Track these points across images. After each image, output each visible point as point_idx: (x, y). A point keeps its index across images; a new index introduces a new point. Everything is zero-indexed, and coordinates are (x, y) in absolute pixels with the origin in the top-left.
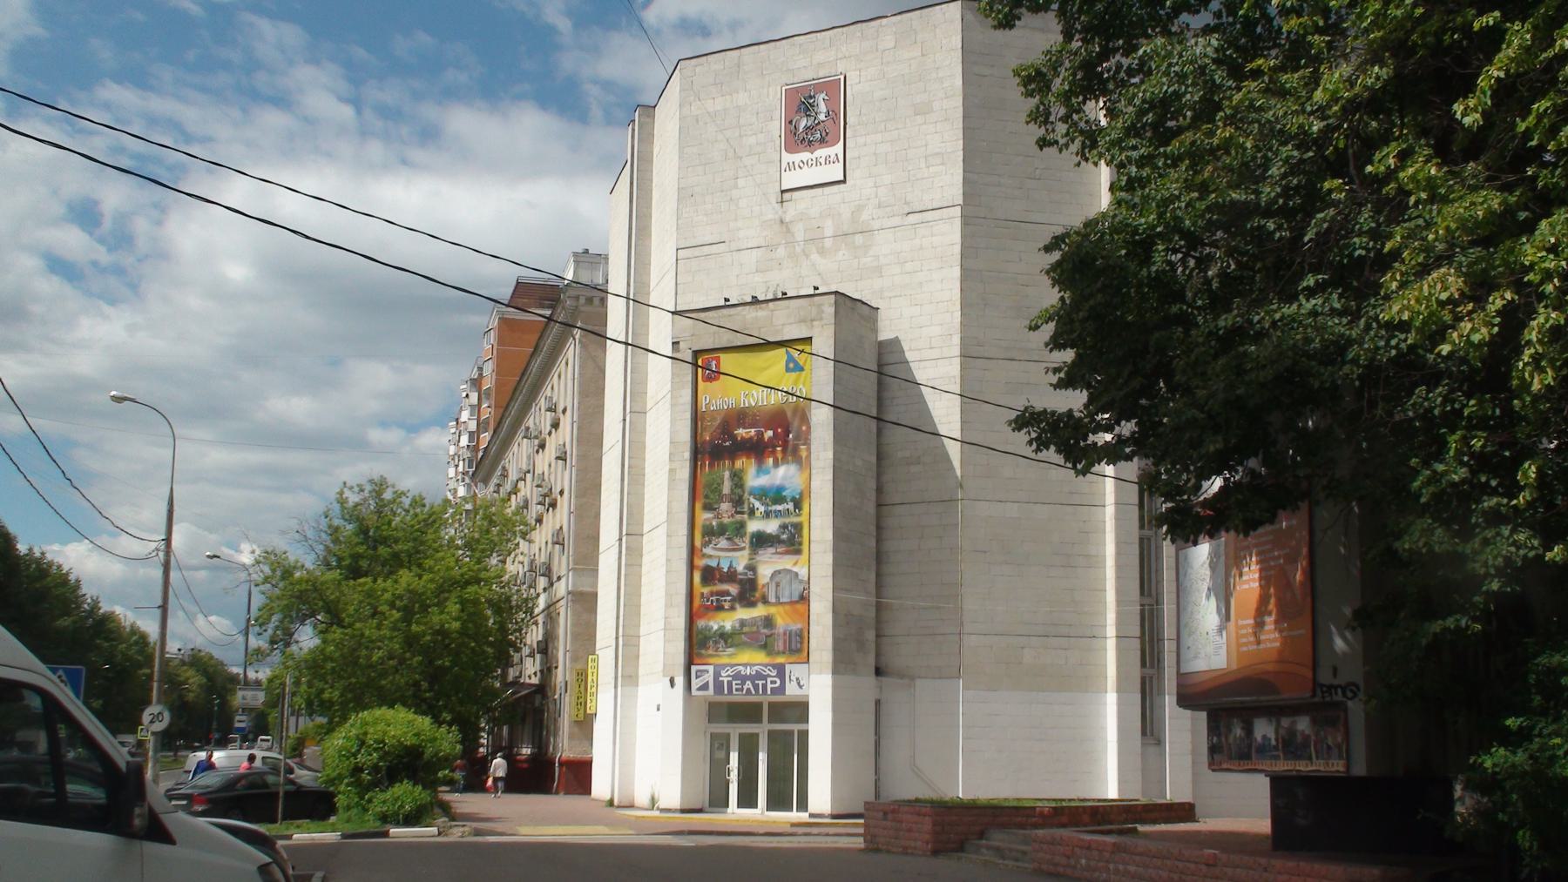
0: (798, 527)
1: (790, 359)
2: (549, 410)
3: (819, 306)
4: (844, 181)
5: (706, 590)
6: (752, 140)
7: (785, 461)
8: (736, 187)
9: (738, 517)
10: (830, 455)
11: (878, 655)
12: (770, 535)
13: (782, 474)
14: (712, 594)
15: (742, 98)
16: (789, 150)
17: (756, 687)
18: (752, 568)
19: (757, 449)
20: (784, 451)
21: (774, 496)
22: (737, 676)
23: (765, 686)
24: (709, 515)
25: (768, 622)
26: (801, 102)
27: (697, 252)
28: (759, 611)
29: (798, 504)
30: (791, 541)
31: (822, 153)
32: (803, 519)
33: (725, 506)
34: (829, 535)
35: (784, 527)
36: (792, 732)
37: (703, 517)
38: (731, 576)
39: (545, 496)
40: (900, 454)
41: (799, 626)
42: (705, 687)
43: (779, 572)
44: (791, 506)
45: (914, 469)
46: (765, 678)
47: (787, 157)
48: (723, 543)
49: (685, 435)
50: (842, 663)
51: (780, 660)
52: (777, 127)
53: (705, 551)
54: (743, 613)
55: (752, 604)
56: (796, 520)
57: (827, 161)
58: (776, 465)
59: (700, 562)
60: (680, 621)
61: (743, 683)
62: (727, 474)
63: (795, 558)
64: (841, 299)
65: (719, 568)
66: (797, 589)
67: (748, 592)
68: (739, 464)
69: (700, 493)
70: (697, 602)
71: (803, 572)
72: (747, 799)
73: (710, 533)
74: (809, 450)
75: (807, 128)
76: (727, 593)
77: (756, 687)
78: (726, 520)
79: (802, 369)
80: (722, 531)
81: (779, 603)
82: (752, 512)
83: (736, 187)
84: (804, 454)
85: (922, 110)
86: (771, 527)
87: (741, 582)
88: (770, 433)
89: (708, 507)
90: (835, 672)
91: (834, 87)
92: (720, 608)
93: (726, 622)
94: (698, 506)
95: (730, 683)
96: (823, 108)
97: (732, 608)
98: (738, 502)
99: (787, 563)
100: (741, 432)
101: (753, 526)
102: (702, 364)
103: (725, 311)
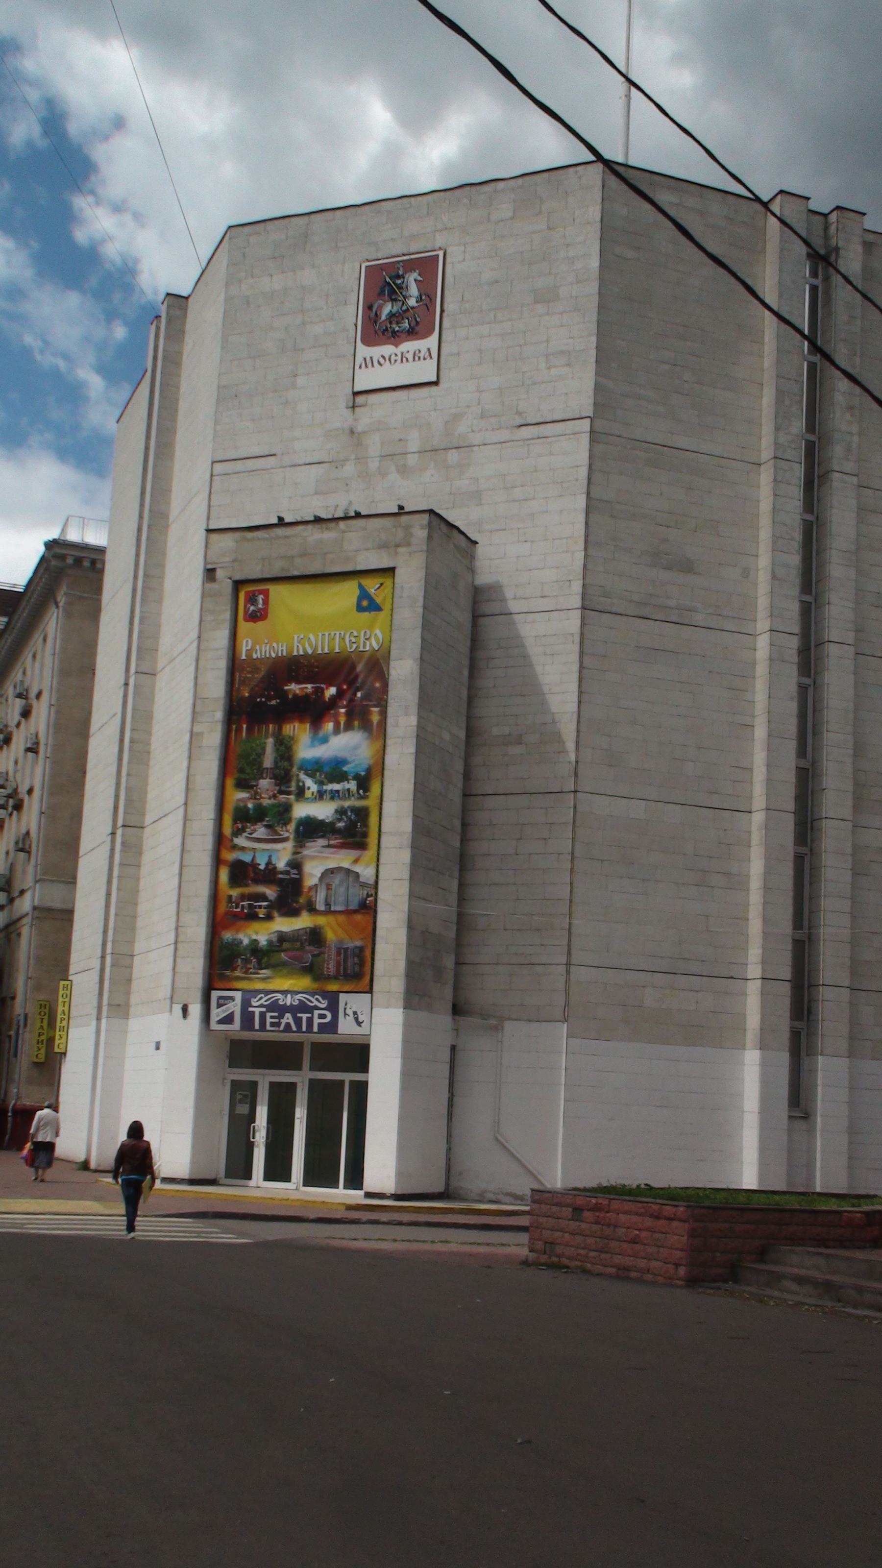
0: (362, 814)
1: (364, 594)
2: (19, 696)
3: (407, 528)
5: (235, 893)
6: (318, 329)
7: (349, 727)
8: (294, 386)
9: (282, 798)
10: (413, 720)
11: (456, 988)
12: (322, 823)
13: (344, 744)
14: (243, 897)
15: (308, 276)
16: (368, 341)
17: (298, 1021)
18: (296, 865)
19: (314, 712)
20: (350, 715)
21: (332, 771)
22: (273, 1007)
23: (310, 1021)
24: (243, 795)
25: (315, 936)
26: (384, 282)
27: (239, 466)
28: (303, 922)
29: (364, 783)
30: (354, 831)
31: (409, 346)
32: (371, 802)
33: (265, 784)
34: (407, 825)
35: (341, 812)
36: (342, 1082)
37: (236, 796)
38: (269, 875)
39: (9, 796)
40: (495, 731)
41: (358, 943)
42: (228, 1019)
43: (331, 871)
44: (352, 785)
45: (514, 750)
46: (310, 1010)
47: (363, 351)
48: (261, 831)
49: (216, 687)
50: (415, 996)
51: (333, 987)
52: (352, 313)
53: (240, 841)
54: (283, 925)
55: (293, 913)
56: (359, 803)
57: (416, 356)
58: (337, 731)
59: (230, 856)
60: (197, 930)
61: (281, 1016)
62: (270, 741)
63: (353, 854)
64: (433, 517)
65: (254, 865)
66: (357, 895)
67: (290, 894)
68: (289, 729)
69: (237, 767)
70: (223, 908)
71: (366, 872)
72: (278, 1169)
73: (245, 818)
74: (384, 714)
75: (391, 315)
76: (263, 897)
77: (298, 1021)
78: (266, 802)
79: (379, 609)
80: (259, 815)
81: (328, 912)
82: (301, 793)
83: (294, 386)
84: (375, 718)
85: (546, 297)
86: (323, 811)
87: (280, 883)
88: (333, 690)
89: (242, 785)
90: (408, 1005)
91: (427, 266)
92: (252, 917)
93: (261, 934)
94: (230, 782)
95: (263, 1016)
96: (414, 290)
97: (269, 918)
98: (283, 777)
99: (343, 859)
100: (294, 688)
101: (301, 811)
102: (248, 596)
103: (280, 531)
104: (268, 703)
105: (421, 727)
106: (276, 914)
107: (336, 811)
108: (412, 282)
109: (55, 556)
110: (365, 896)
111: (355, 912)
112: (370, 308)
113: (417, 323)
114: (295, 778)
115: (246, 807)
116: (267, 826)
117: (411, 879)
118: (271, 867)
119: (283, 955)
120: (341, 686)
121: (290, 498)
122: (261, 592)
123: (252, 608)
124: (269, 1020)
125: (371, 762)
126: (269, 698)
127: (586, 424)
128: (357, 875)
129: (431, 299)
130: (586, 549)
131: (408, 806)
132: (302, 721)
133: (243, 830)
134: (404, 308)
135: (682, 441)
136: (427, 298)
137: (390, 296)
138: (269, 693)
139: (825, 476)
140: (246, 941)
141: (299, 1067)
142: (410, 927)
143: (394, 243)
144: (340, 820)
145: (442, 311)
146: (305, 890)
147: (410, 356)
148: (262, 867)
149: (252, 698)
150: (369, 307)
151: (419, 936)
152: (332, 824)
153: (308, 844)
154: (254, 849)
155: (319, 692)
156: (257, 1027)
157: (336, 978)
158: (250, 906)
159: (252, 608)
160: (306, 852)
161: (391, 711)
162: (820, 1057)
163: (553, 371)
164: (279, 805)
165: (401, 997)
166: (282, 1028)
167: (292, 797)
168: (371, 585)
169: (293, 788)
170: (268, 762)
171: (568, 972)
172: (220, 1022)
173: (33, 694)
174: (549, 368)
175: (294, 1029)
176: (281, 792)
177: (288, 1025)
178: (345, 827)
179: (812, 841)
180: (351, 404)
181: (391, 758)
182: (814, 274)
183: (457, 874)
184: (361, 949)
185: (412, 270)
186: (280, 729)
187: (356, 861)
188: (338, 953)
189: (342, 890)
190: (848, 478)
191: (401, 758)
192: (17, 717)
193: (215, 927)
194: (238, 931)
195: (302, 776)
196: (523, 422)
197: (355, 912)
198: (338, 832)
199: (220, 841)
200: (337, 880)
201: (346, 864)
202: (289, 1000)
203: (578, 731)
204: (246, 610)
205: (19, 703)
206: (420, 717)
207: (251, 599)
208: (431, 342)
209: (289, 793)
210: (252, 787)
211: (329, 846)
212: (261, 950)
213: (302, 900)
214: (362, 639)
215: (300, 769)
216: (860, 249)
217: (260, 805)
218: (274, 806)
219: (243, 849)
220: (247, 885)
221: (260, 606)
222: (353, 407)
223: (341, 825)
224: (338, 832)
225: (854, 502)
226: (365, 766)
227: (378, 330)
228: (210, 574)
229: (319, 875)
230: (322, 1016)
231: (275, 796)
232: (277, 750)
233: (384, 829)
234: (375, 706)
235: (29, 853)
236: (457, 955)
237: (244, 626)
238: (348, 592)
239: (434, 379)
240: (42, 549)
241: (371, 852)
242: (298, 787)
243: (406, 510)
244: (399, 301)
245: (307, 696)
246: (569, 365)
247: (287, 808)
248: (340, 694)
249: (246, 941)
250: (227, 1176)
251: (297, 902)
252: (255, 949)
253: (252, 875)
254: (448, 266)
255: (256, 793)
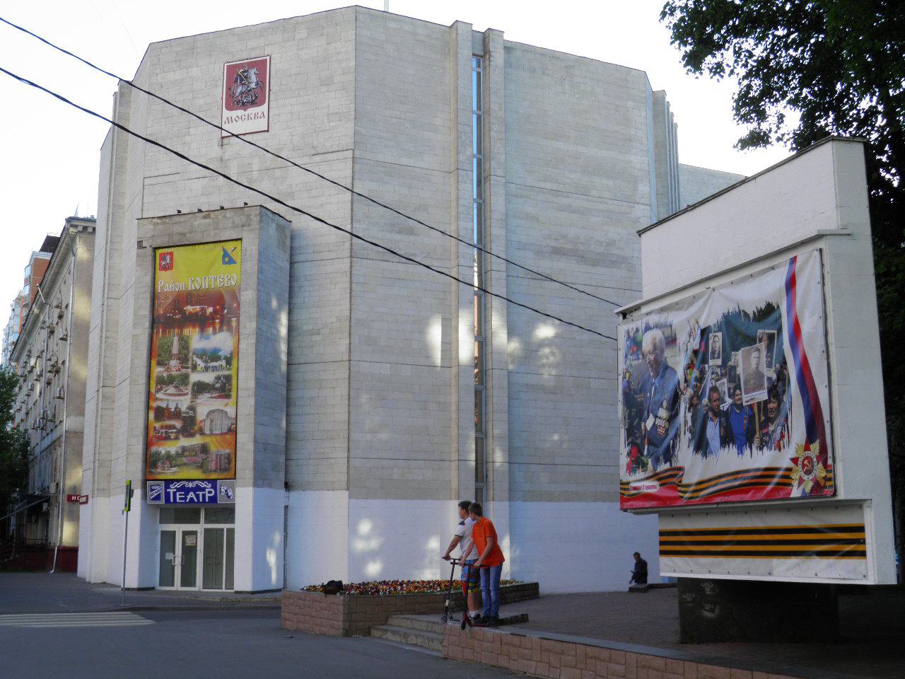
0: (228, 378)
1: (226, 254)
2: (57, 307)
3: (248, 216)
4: (268, 131)
5: (157, 425)
6: (201, 102)
7: (221, 329)
8: (189, 134)
9: (184, 371)
10: (254, 325)
11: (286, 473)
12: (208, 384)
14: (162, 427)
15: (195, 72)
16: (229, 108)
17: (197, 496)
18: (192, 408)
19: (203, 322)
20: (221, 323)
21: (213, 356)
22: (183, 489)
23: (204, 496)
24: (160, 369)
25: (204, 449)
26: (236, 75)
27: (159, 180)
28: (197, 440)
29: (229, 361)
30: (224, 389)
31: (252, 111)
32: (233, 372)
33: (174, 363)
34: (252, 384)
35: (218, 378)
36: (222, 530)
37: (157, 370)
38: (177, 414)
39: (53, 366)
40: (305, 328)
41: (227, 451)
42: (158, 498)
43: (213, 411)
44: (223, 363)
45: (316, 338)
46: (204, 489)
47: (227, 114)
48: (171, 390)
50: (260, 480)
51: (213, 476)
52: (220, 92)
53: (159, 395)
54: (185, 442)
55: (192, 435)
56: (226, 373)
57: (256, 116)
58: (215, 333)
59: (154, 404)
60: (139, 448)
61: (187, 494)
62: (176, 339)
63: (226, 401)
64: (263, 209)
65: (167, 409)
66: (226, 424)
67: (189, 425)
68: (186, 332)
69: (155, 353)
70: (152, 433)
71: (231, 411)
72: (188, 579)
73: (162, 382)
74: (238, 322)
75: (242, 93)
76: (174, 427)
77: (197, 496)
78: (174, 373)
79: (235, 262)
80: (170, 381)
81: (212, 434)
82: (194, 367)
83: (189, 134)
84: (234, 324)
85: (326, 83)
86: (208, 378)
87: (184, 419)
88: (210, 310)
89: (160, 364)
90: (256, 485)
91: (261, 66)
92: (167, 438)
93: (171, 447)
94: (154, 363)
95: (175, 494)
96: (254, 79)
97: (177, 438)
98: (184, 359)
99: (219, 404)
100: (189, 308)
101: (194, 377)
102: (159, 255)
103: (177, 219)
104: (172, 317)
105: (259, 329)
106: (181, 436)
107: (215, 378)
108: (253, 74)
109: (72, 226)
110: (230, 425)
111: (226, 433)
112: (230, 89)
113: (256, 98)
114: (191, 359)
115: (162, 376)
116: (175, 387)
117: (256, 414)
118: (178, 410)
119: (184, 459)
120: (214, 309)
121: (188, 198)
122: (168, 254)
123: (163, 263)
124: (178, 497)
125: (232, 349)
126: (175, 314)
127: (350, 154)
128: (226, 413)
129: (264, 84)
130: (352, 223)
131: (252, 374)
132: (194, 327)
133: (161, 389)
134: (249, 89)
135: (405, 161)
136: (261, 83)
137: (241, 82)
138: (175, 311)
139: (487, 178)
140: (163, 452)
141: (197, 522)
142: (256, 442)
143: (242, 54)
144: (217, 383)
145: (270, 90)
146: (198, 423)
147: (252, 116)
148: (173, 410)
149: (164, 314)
150: (229, 89)
151: (261, 446)
152: (213, 385)
153: (199, 397)
154: (168, 400)
155: (203, 310)
156: (172, 501)
157: (215, 471)
158: (166, 432)
159: (163, 263)
160: (198, 401)
161: (241, 319)
162: (492, 502)
163: (332, 124)
164: (182, 375)
165: (252, 481)
166: (188, 501)
167: (189, 370)
168: (229, 247)
169: (190, 364)
170: (175, 350)
171: (348, 461)
172: (153, 499)
173: (64, 306)
174: (329, 122)
175: (196, 500)
176: (183, 368)
177: (192, 499)
178: (7, 432)
179: (486, 382)
180: (220, 144)
181: (243, 346)
182: (479, 66)
183: (285, 409)
184: (229, 455)
185: (253, 68)
186: (182, 331)
187: (226, 405)
188: (217, 458)
189: (219, 422)
190: (500, 179)
191: (248, 347)
192: (56, 319)
193: (148, 444)
194: (159, 446)
195: (195, 358)
196: (316, 153)
197: (226, 433)
198: (217, 389)
199: (149, 395)
200: (216, 416)
201: (221, 408)
202: (190, 485)
203: (350, 327)
204: (160, 265)
205: (57, 311)
206: (258, 323)
207: (163, 257)
208: (264, 108)
209: (187, 368)
210: (166, 365)
211: (212, 397)
212: (172, 456)
213: (196, 428)
214: (226, 280)
215: (194, 354)
216: (502, 51)
217: (170, 375)
218: (179, 375)
219: (161, 400)
220: (165, 420)
221: (168, 262)
222: (222, 145)
223: (218, 385)
224: (217, 389)
225: (503, 192)
226: (229, 352)
227: (234, 102)
228: (140, 245)
229: (206, 414)
230: (210, 492)
231: (179, 370)
232: (180, 344)
233: (239, 387)
234: (234, 317)
235: (63, 399)
236: (287, 454)
237: (160, 274)
238: (217, 251)
239: (267, 129)
240: (63, 223)
241: (233, 400)
242: (193, 365)
243: (249, 205)
244: (247, 86)
245: (196, 314)
246: (340, 120)
247: (186, 377)
248: (215, 311)
249: (163, 452)
250: (161, 585)
251: (193, 429)
252: (168, 457)
253: (167, 414)
254: (272, 65)
255: (168, 368)
